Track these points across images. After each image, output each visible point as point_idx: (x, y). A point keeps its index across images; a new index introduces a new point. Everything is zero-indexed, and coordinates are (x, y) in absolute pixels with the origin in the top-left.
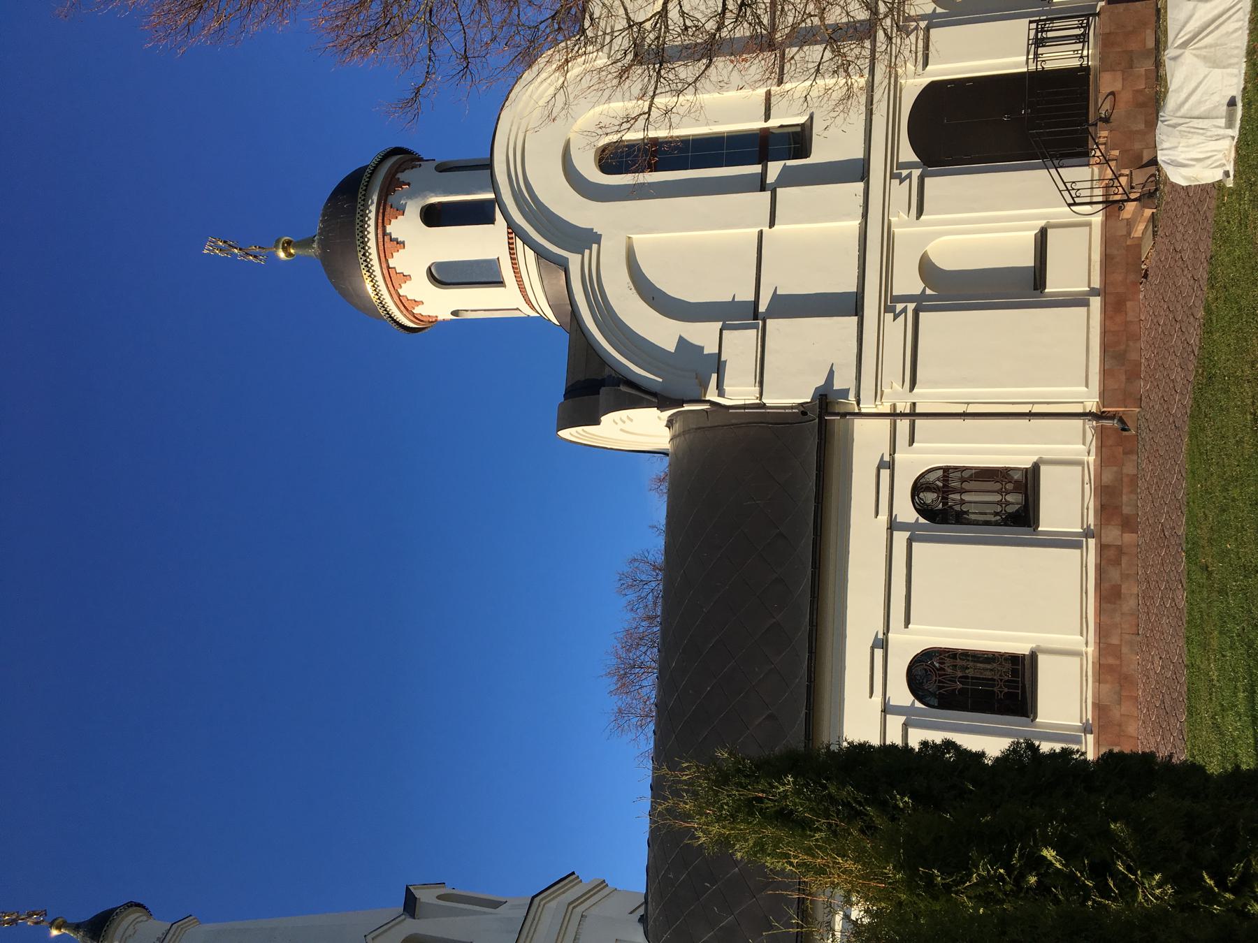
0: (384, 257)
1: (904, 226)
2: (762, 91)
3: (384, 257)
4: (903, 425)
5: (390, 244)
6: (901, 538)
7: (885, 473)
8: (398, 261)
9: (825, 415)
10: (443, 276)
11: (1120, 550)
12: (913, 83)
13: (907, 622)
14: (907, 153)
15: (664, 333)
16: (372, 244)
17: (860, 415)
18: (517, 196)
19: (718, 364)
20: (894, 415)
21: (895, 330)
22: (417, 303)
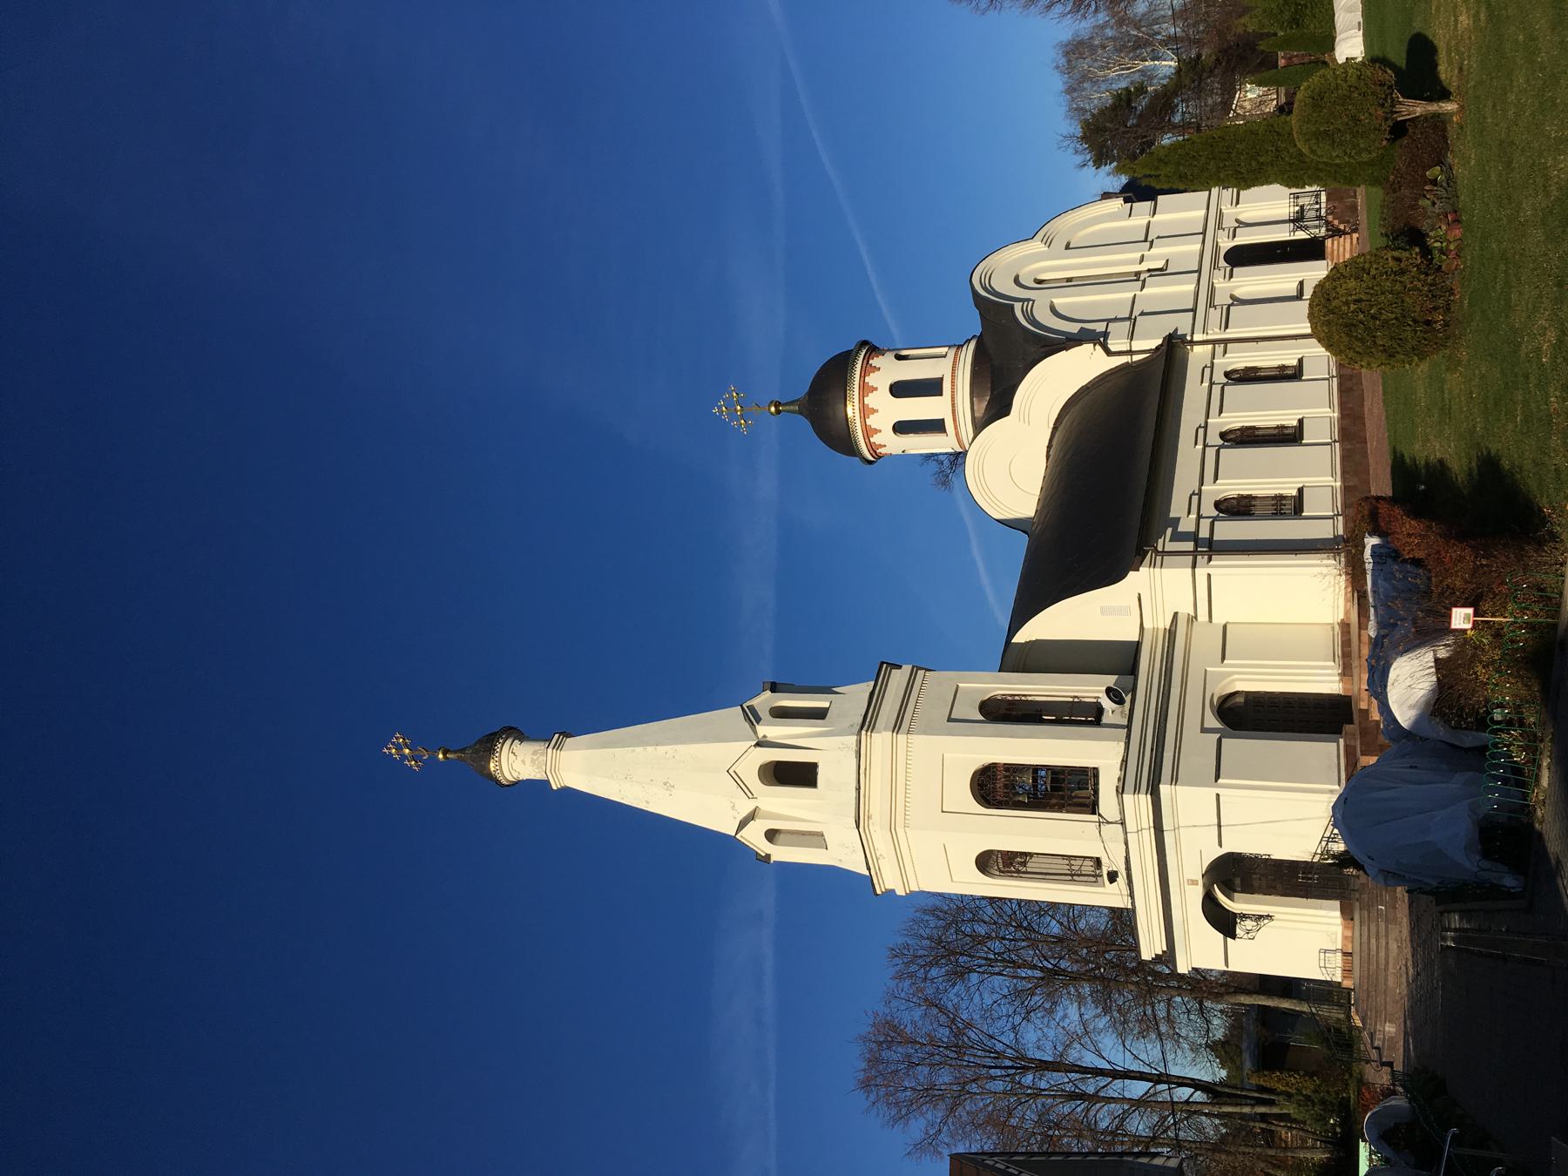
0: (864, 374)
1: (1220, 283)
2: (1139, 255)
3: (864, 374)
4: (1220, 348)
5: (868, 369)
6: (1216, 390)
7: (1207, 371)
8: (871, 379)
9: (1174, 347)
10: (900, 390)
11: (1351, 377)
12: (1226, 244)
13: (1221, 412)
14: (1222, 263)
15: (1074, 328)
16: (859, 366)
17: (1192, 343)
18: (985, 289)
19: (1106, 334)
20: (1214, 342)
21: (1215, 315)
22: (874, 411)
